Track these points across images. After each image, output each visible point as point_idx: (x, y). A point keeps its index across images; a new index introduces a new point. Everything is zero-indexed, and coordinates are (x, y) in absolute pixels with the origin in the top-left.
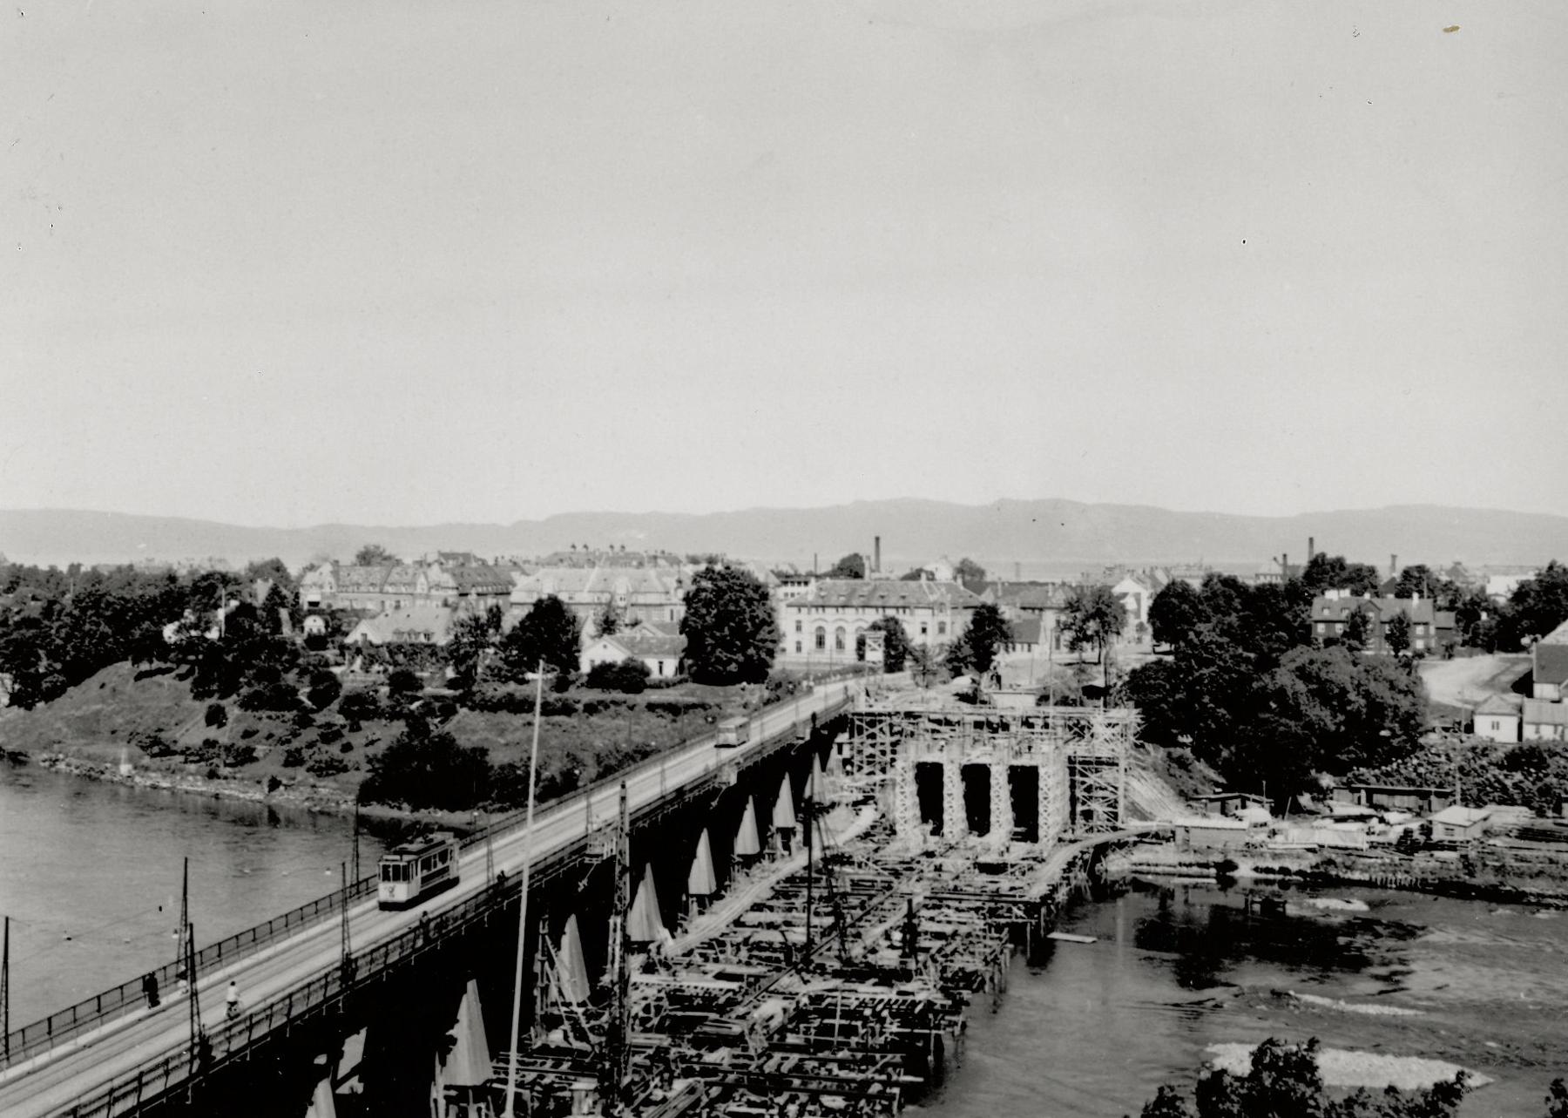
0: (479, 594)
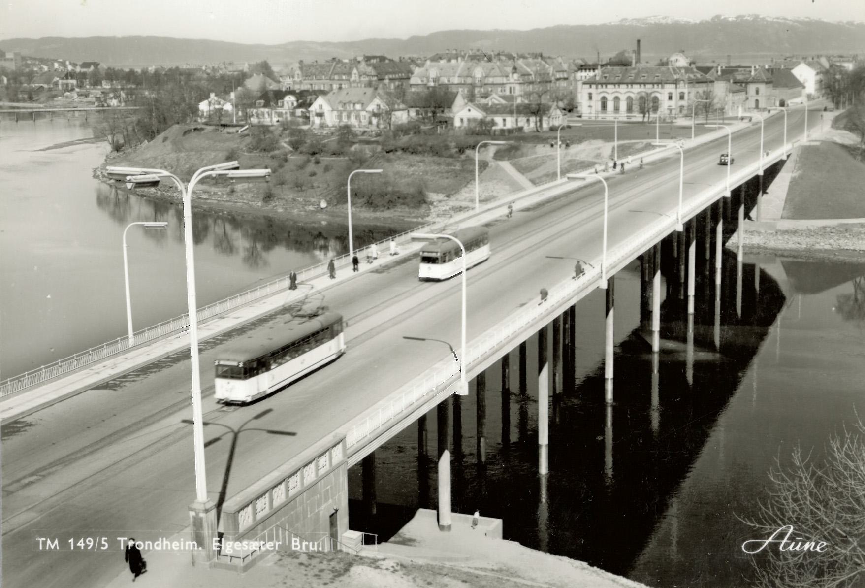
0: (390, 79)
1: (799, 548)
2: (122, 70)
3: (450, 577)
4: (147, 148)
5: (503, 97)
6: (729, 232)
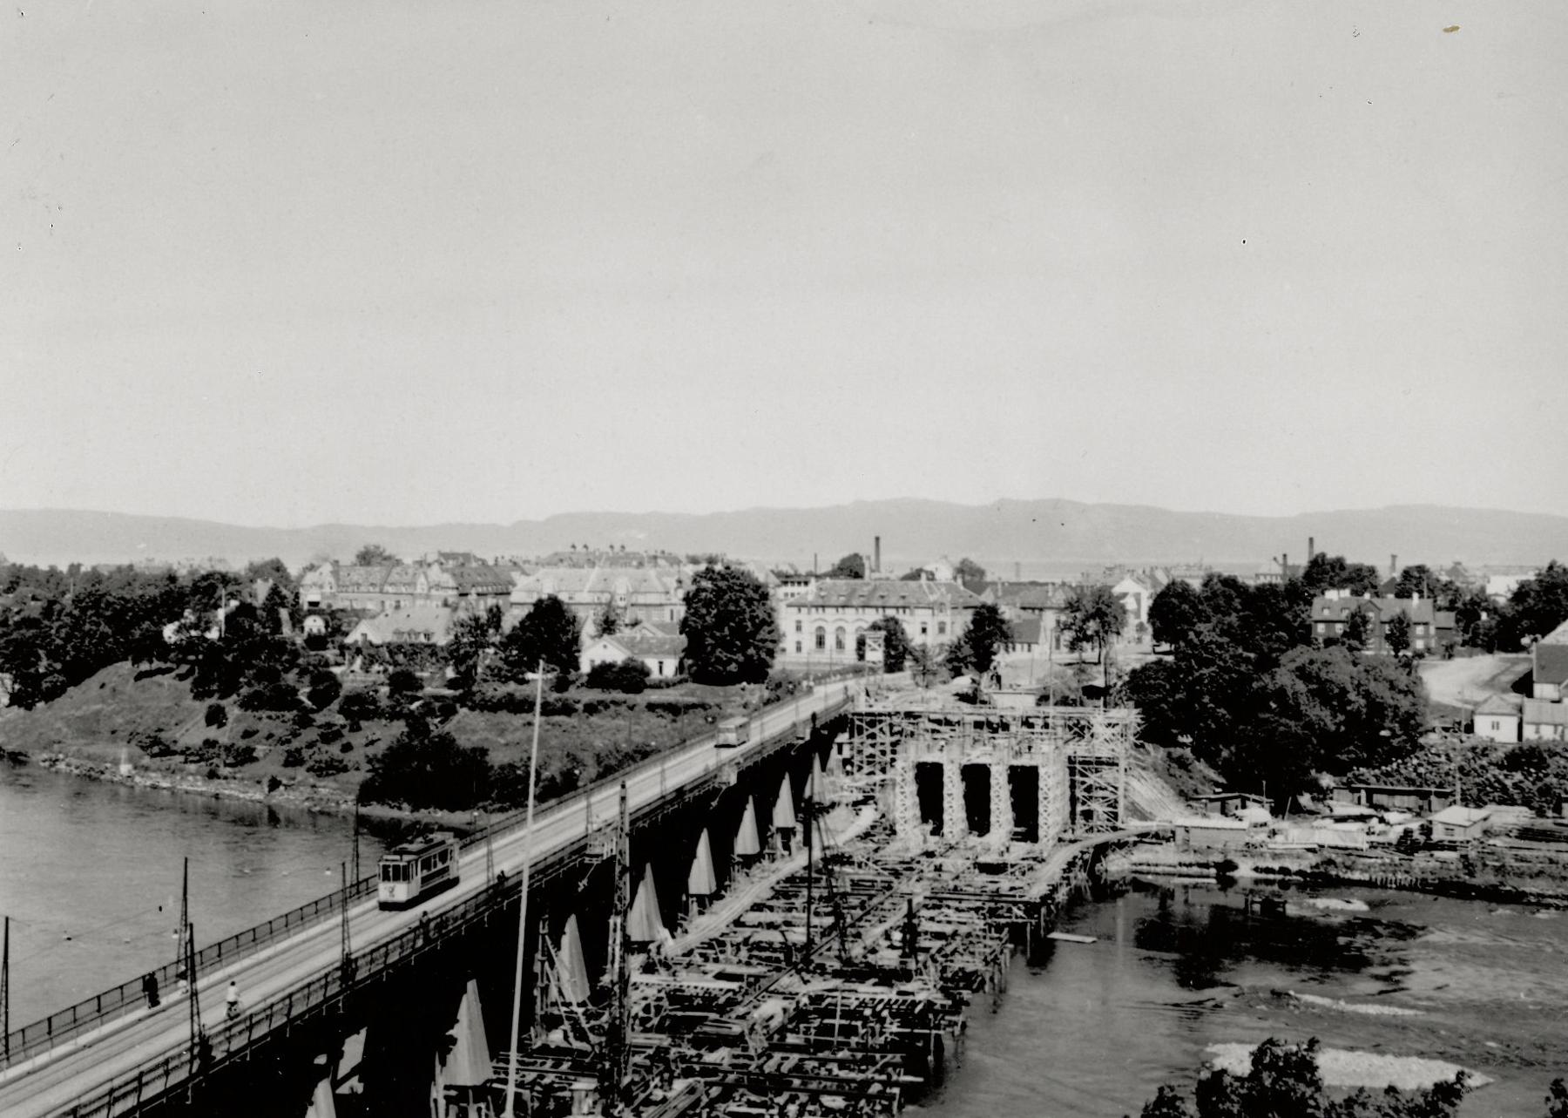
0: (478, 594)
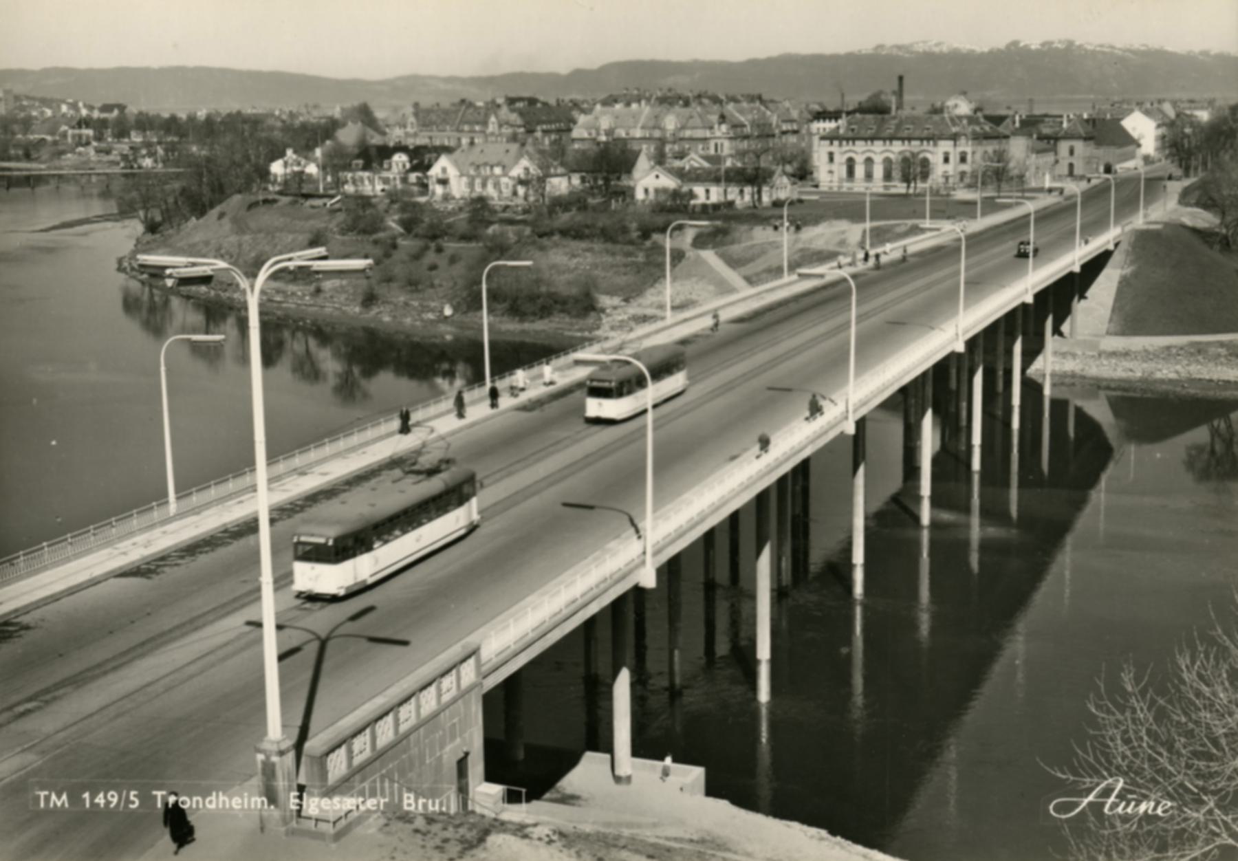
1: (1133, 810)
2: (158, 116)
3: (630, 850)
4: (195, 228)
5: (707, 158)
6: (1030, 355)
